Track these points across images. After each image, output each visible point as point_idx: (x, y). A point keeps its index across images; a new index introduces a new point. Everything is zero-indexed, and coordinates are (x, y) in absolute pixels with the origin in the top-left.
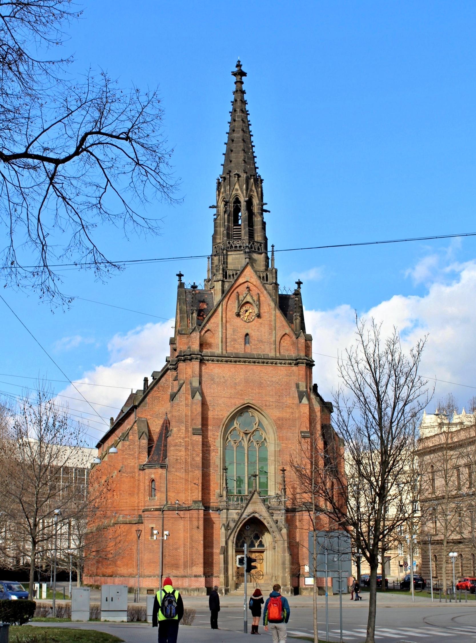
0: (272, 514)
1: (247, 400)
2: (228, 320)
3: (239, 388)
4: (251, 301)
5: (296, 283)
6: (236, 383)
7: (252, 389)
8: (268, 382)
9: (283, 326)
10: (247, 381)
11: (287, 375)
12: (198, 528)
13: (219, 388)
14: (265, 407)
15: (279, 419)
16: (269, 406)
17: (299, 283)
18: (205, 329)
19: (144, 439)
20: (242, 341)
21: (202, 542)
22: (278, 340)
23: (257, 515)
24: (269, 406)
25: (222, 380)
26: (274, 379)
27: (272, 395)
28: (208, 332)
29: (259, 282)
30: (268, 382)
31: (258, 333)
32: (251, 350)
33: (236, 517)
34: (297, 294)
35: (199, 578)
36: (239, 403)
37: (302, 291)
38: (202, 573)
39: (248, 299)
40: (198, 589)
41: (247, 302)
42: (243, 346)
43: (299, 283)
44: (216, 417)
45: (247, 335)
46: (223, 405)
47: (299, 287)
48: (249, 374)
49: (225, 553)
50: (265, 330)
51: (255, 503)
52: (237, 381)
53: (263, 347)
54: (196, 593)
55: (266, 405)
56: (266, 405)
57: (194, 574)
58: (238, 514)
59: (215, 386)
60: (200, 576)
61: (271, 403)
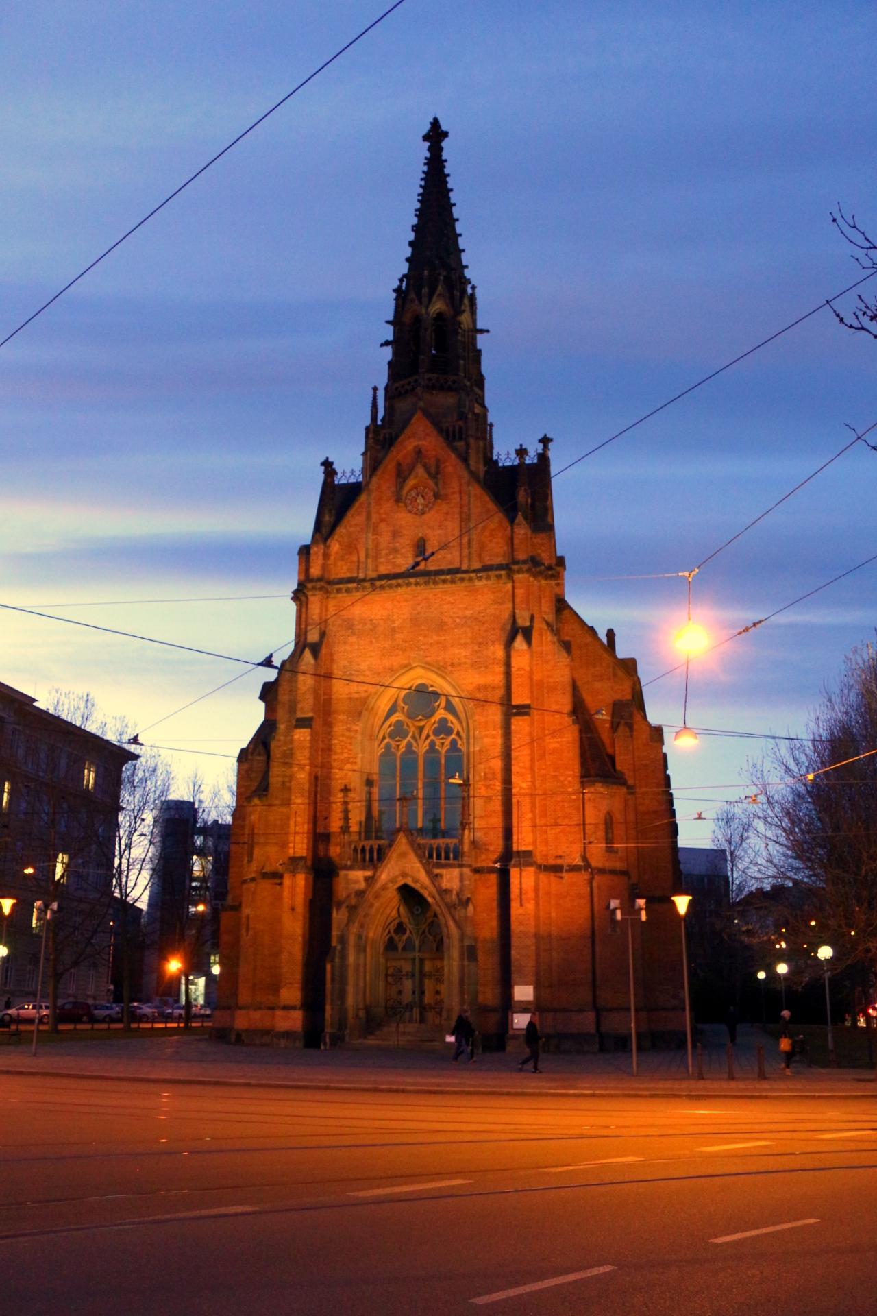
5: (540, 441)
6: (394, 630)
7: (425, 636)
9: (488, 511)
10: (415, 621)
12: (293, 909)
13: (362, 642)
14: (450, 668)
15: (479, 688)
16: (460, 664)
17: (545, 441)
19: (259, 754)
21: (300, 939)
24: (460, 664)
25: (368, 626)
26: (468, 613)
27: (465, 644)
31: (439, 532)
33: (363, 885)
34: (543, 459)
35: (292, 1012)
37: (551, 454)
38: (298, 1003)
40: (287, 1035)
43: (545, 441)
44: (356, 696)
46: (368, 673)
47: (546, 447)
48: (419, 608)
49: (337, 960)
51: (403, 855)
52: (397, 624)
54: (283, 1043)
55: (452, 665)
56: (452, 665)
57: (282, 1004)
58: (367, 879)
59: (354, 639)
60: (293, 1008)
61: (463, 660)
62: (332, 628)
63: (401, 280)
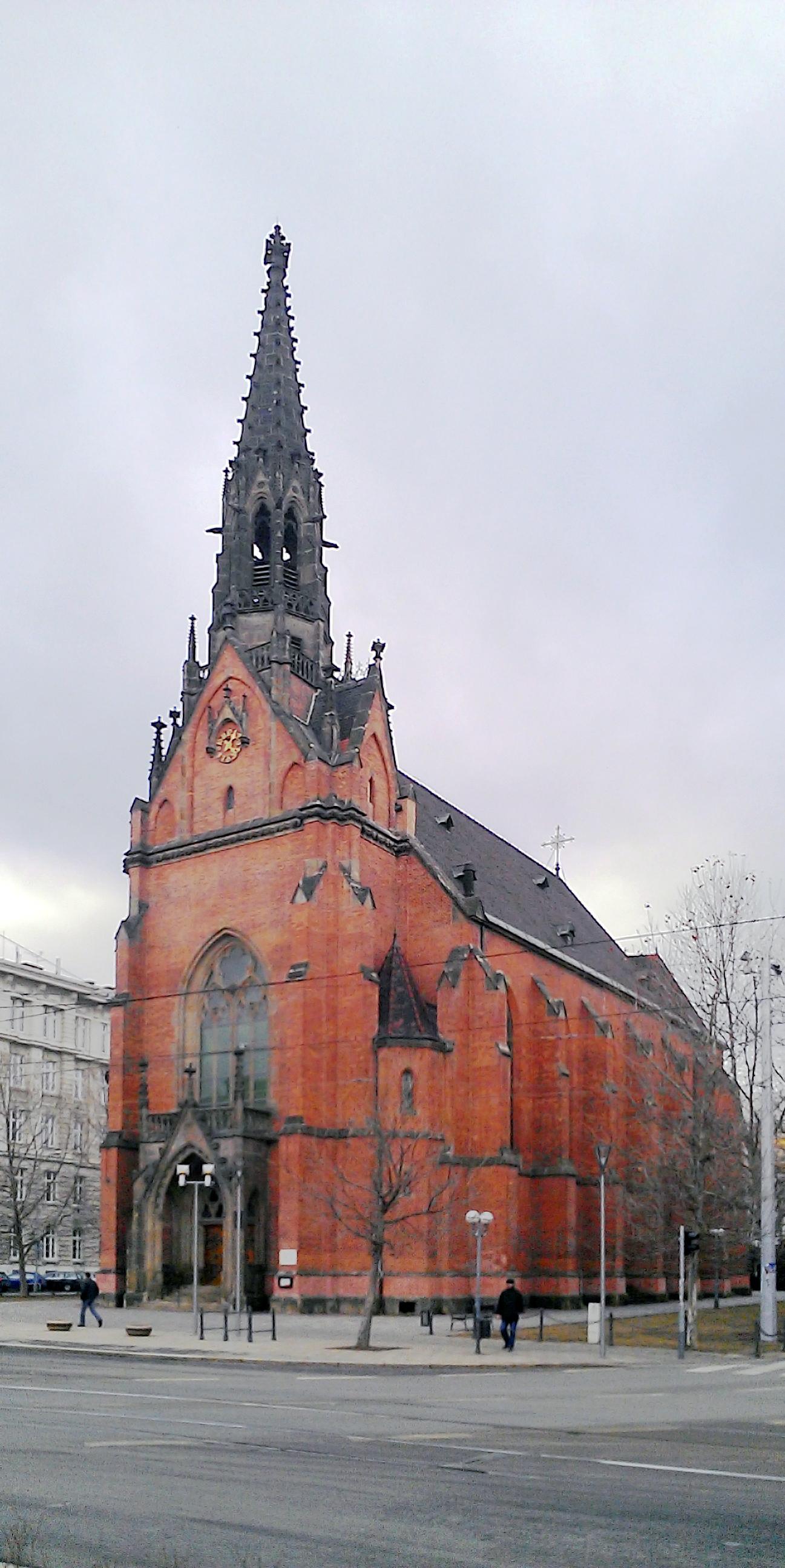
0: (217, 1147)
1: (221, 922)
2: (197, 769)
3: (209, 902)
4: (231, 716)
8: (258, 877)
11: (292, 853)
15: (278, 949)
16: (260, 925)
18: (158, 800)
20: (219, 806)
22: (277, 781)
23: (197, 1152)
24: (260, 925)
26: (268, 868)
28: (166, 805)
29: (245, 672)
30: (258, 877)
32: (239, 818)
36: (208, 930)
39: (228, 714)
41: (228, 721)
42: (220, 816)
45: (231, 788)
50: (258, 767)
51: (189, 1125)
53: (254, 806)
62: (152, 901)
63: (226, 471)
